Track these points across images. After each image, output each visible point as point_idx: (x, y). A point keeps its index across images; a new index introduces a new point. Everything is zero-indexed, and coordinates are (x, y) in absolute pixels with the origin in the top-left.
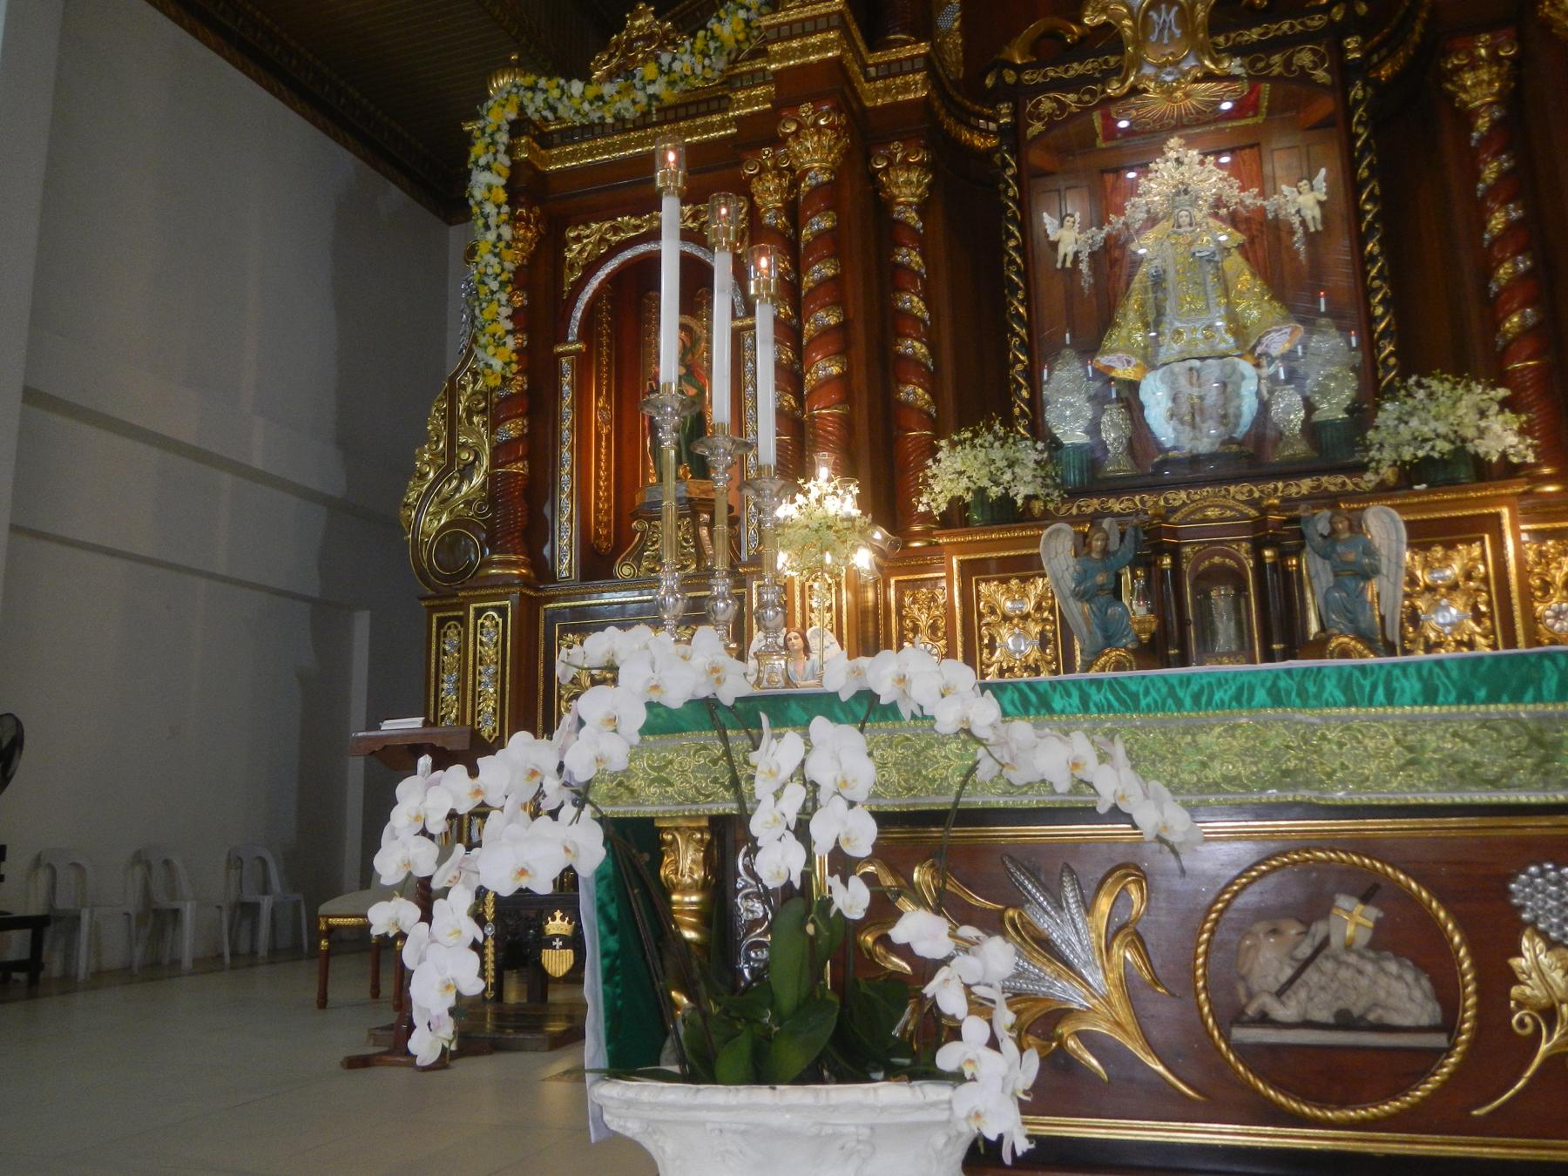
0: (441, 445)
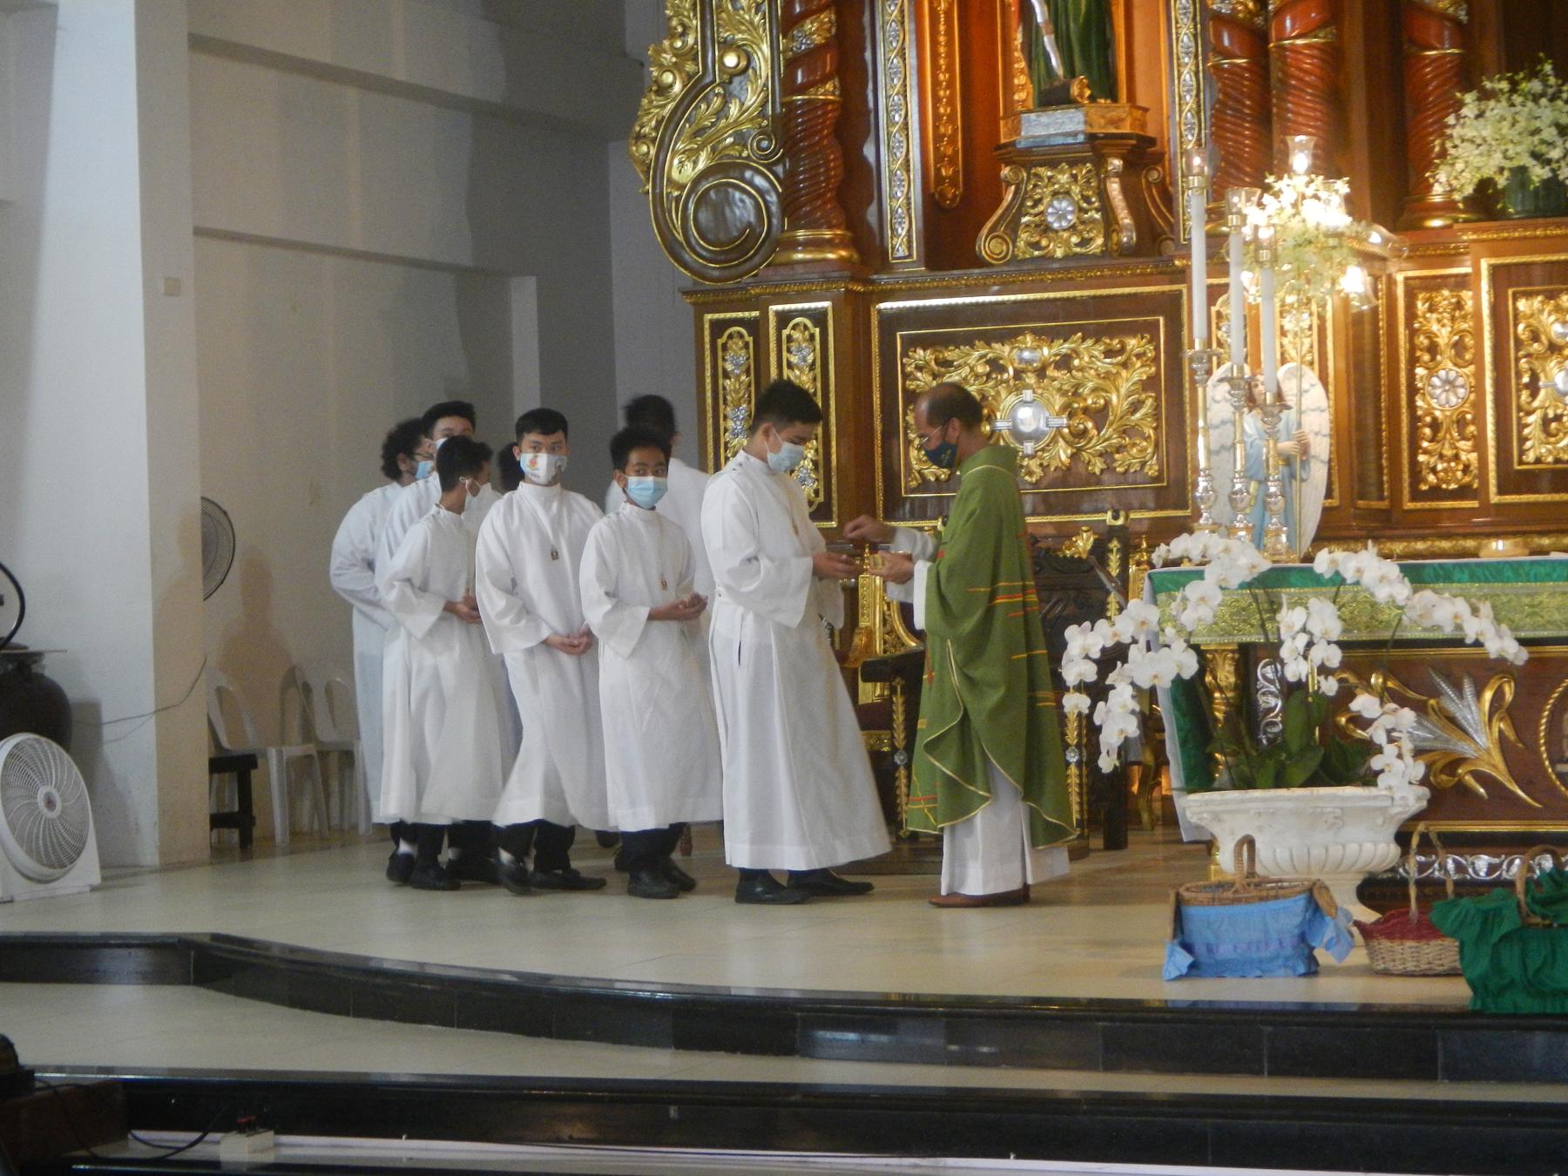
0: (691, 40)
